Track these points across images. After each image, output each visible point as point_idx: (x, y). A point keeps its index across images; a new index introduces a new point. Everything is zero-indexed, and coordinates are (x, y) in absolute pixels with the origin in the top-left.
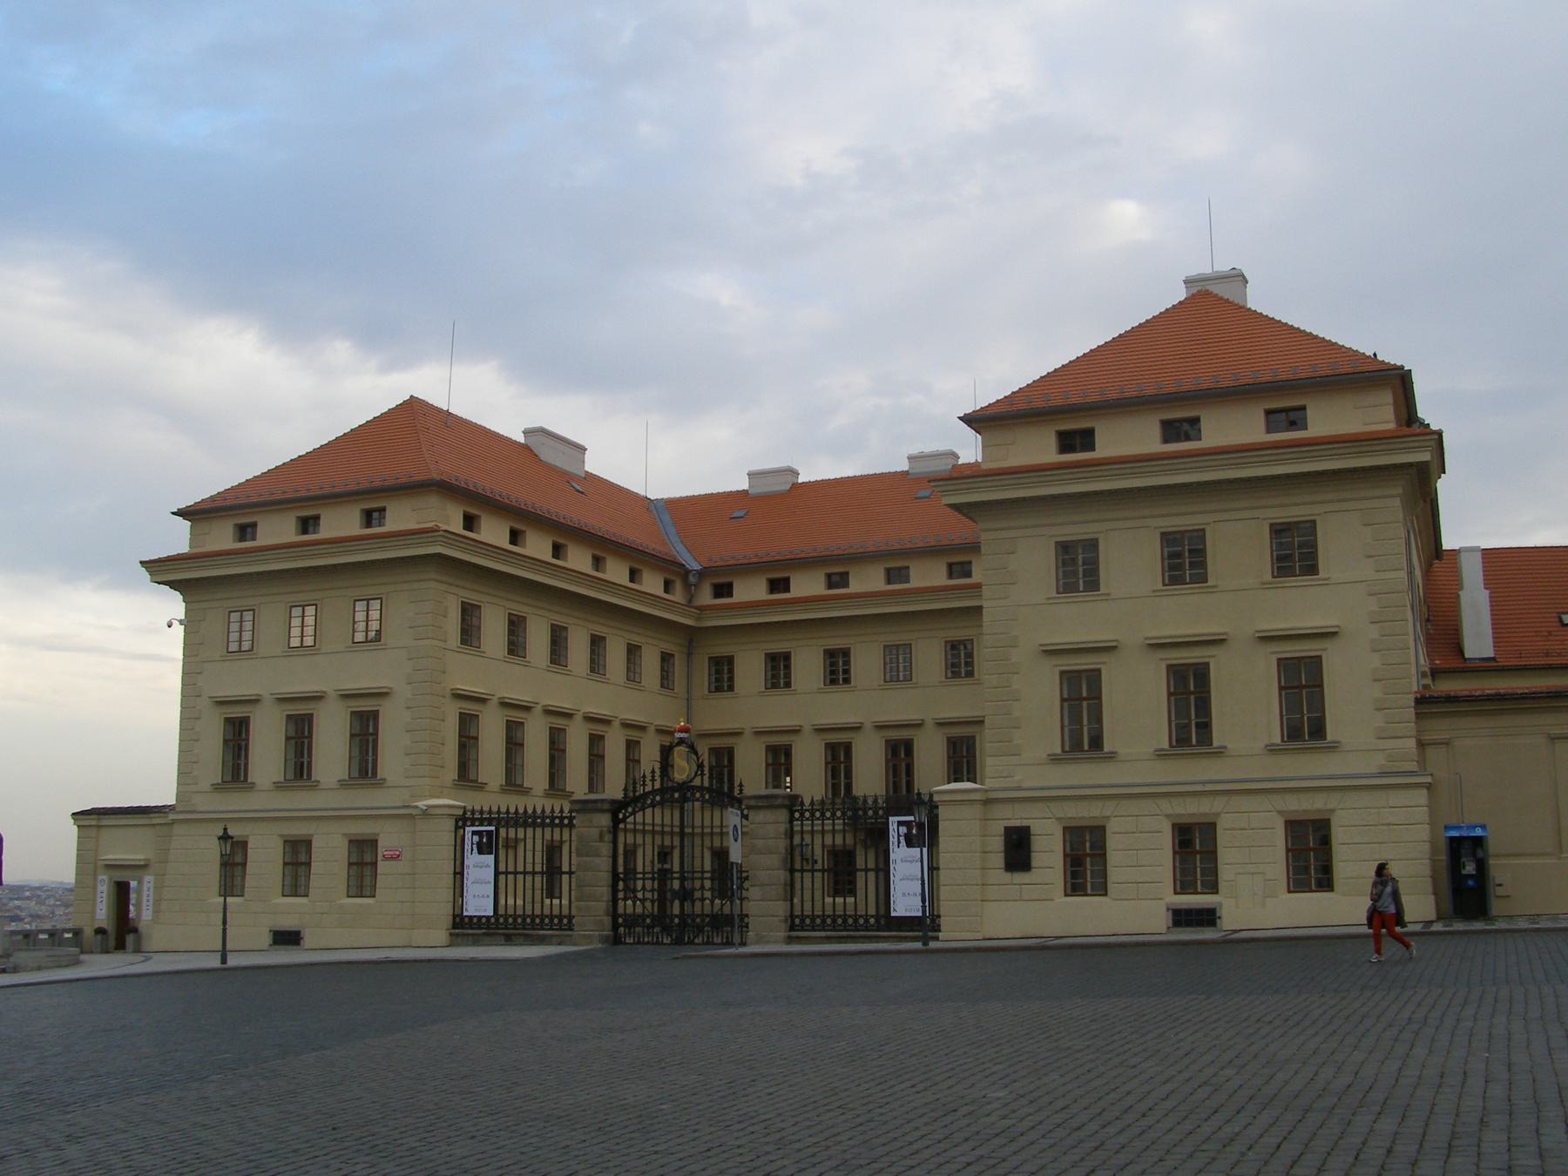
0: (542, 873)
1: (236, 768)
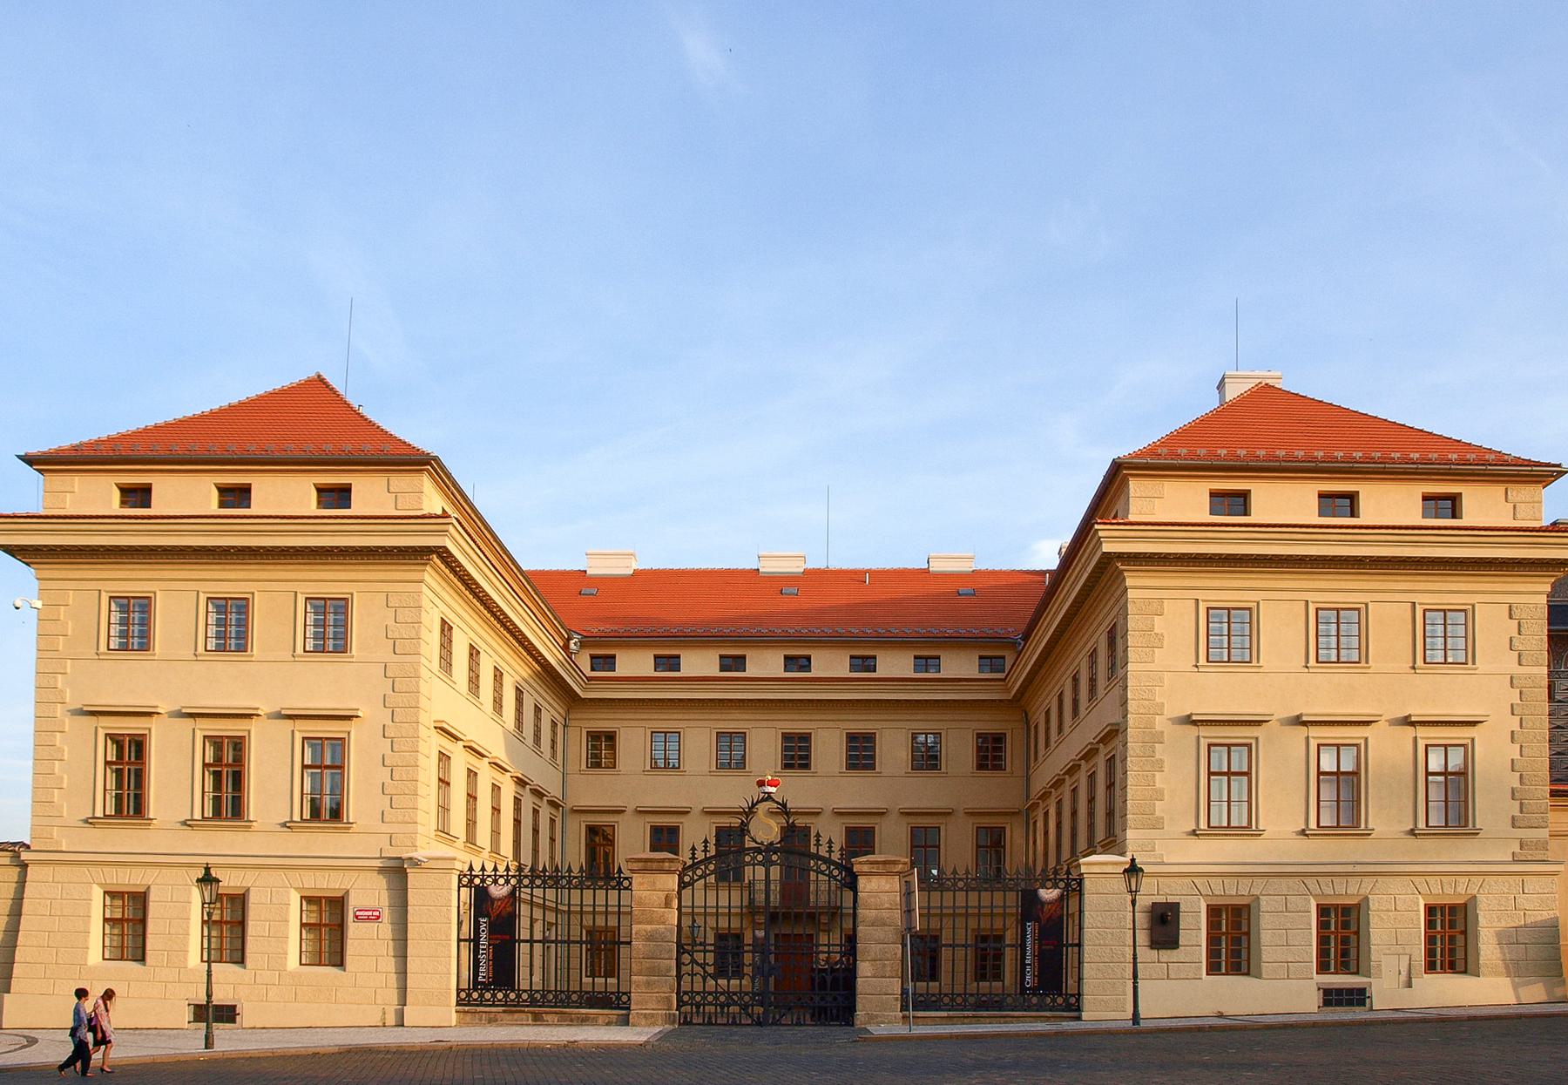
0: (469, 940)
1: (130, 800)
